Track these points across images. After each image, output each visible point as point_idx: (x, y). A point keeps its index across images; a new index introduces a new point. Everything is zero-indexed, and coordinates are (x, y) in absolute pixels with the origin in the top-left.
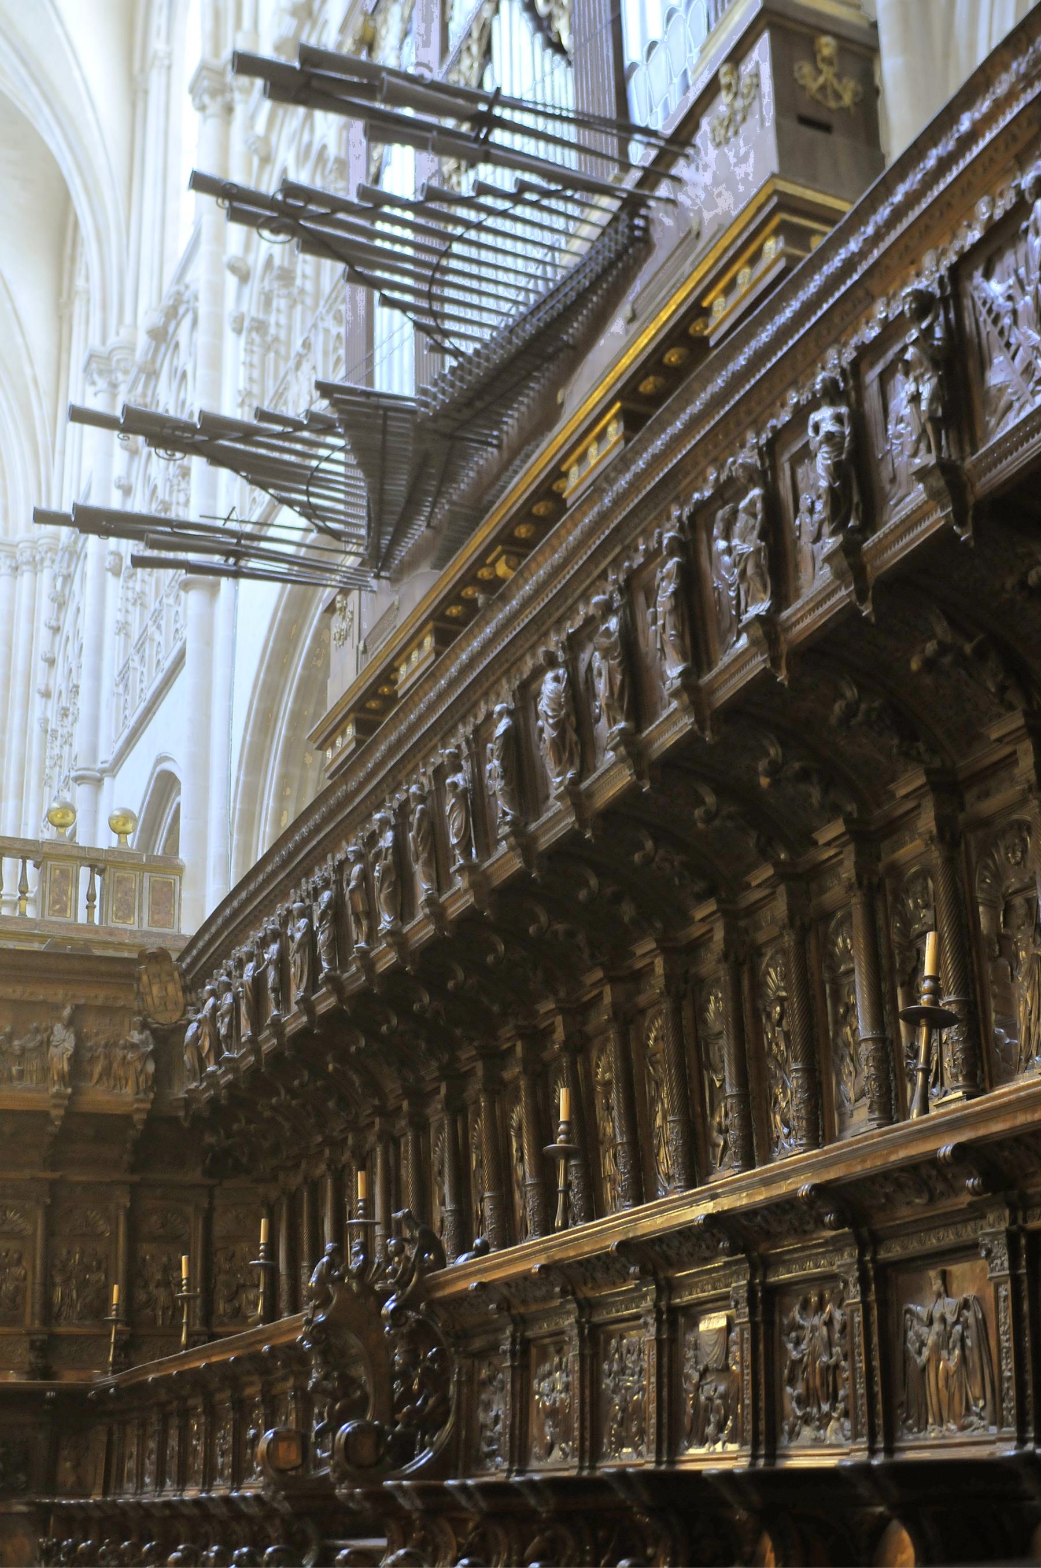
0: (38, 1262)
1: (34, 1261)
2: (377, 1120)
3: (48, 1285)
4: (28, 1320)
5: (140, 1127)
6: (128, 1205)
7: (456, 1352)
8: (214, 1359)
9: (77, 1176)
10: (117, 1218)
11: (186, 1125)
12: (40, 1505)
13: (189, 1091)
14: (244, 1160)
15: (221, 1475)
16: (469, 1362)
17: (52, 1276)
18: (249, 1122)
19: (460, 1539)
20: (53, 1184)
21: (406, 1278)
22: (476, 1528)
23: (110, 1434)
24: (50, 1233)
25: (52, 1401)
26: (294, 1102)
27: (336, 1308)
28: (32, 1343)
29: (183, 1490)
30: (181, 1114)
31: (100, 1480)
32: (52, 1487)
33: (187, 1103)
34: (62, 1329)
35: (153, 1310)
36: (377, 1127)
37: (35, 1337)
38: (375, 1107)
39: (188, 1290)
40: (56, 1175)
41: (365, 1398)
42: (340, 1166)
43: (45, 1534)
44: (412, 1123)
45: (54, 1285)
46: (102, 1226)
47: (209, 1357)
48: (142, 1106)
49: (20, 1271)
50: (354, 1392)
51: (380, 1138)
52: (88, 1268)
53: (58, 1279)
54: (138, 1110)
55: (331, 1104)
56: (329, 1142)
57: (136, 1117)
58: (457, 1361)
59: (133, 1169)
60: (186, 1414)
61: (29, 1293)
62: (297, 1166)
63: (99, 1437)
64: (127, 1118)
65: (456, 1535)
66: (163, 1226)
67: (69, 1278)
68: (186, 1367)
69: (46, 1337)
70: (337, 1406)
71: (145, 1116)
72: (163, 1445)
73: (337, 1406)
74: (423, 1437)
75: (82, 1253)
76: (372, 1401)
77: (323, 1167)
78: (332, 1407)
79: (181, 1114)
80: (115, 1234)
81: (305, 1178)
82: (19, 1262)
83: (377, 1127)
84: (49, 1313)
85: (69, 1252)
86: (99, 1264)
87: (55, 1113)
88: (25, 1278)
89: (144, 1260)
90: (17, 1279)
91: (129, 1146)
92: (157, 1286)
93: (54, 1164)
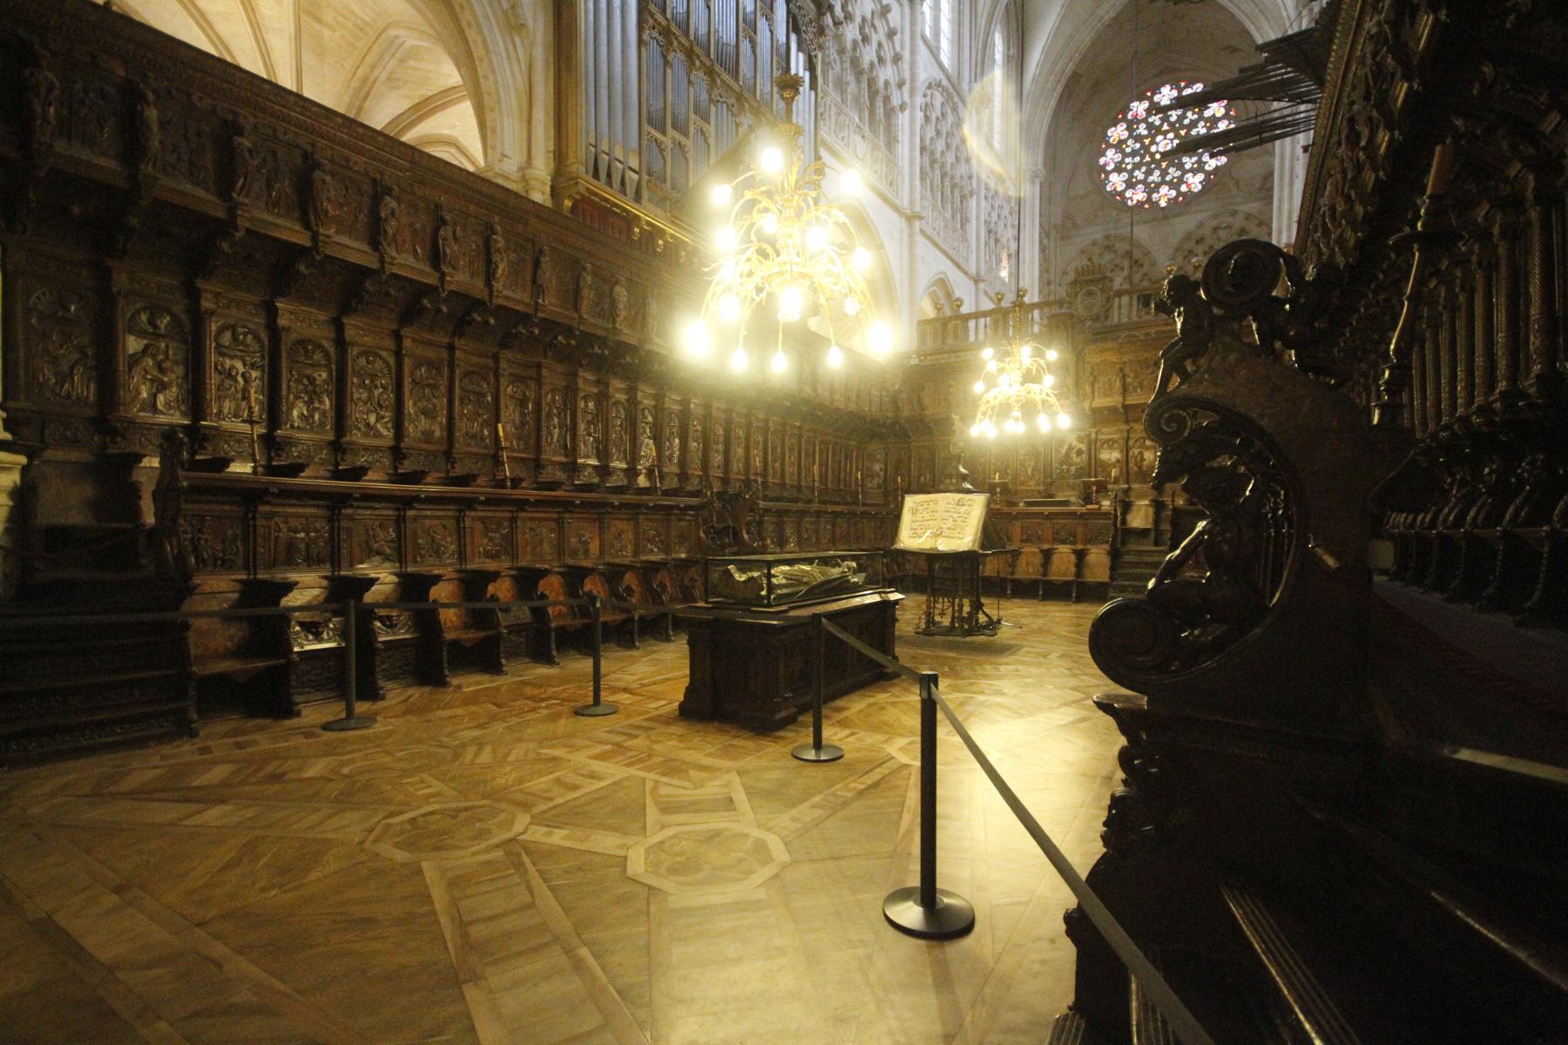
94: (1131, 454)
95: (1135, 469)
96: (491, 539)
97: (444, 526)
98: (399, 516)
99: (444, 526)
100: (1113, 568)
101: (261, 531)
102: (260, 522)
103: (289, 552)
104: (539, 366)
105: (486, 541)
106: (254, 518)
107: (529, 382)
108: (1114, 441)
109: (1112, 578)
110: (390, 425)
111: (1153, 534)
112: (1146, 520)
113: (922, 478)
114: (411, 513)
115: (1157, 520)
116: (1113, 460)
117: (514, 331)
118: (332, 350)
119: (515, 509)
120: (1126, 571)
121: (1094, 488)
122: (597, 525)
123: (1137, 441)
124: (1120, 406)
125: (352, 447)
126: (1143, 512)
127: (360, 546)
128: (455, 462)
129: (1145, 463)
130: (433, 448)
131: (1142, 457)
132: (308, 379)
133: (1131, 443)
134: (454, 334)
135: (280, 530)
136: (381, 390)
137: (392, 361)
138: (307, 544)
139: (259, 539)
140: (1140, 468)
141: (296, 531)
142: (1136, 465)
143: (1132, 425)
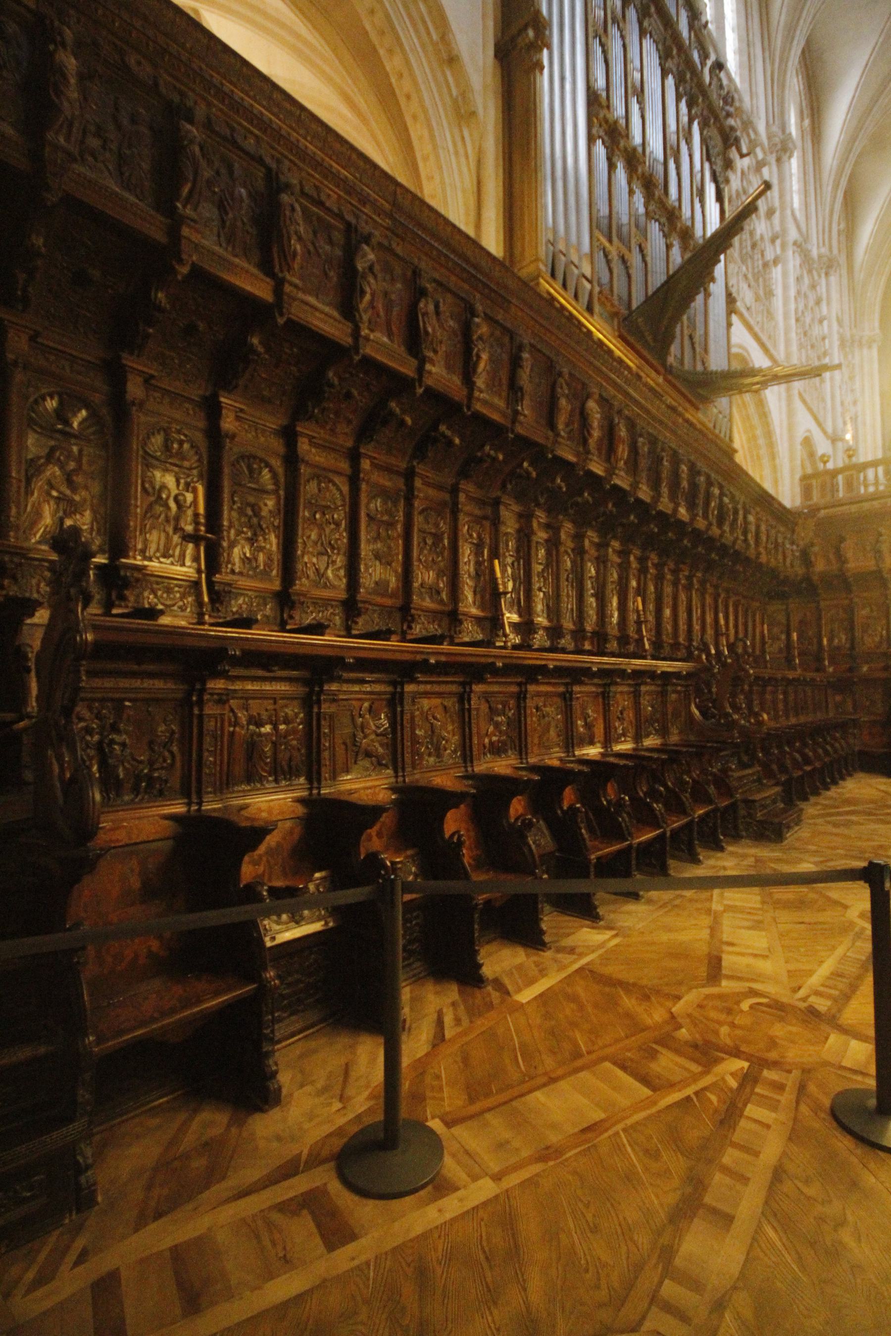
96: (497, 725)
97: (445, 707)
98: (393, 694)
99: (445, 707)
101: (209, 725)
102: (210, 709)
103: (249, 758)
104: (497, 503)
105: (491, 729)
106: (201, 703)
107: (484, 522)
110: (342, 573)
113: (836, 641)
114: (409, 688)
117: (479, 454)
118: (280, 471)
119: (568, 680)
122: (601, 700)
125: (302, 599)
127: (345, 743)
128: (413, 620)
130: (388, 602)
132: (253, 510)
134: (413, 457)
135: (236, 724)
136: (333, 526)
137: (345, 489)
138: (274, 744)
139: (207, 740)
141: (260, 724)
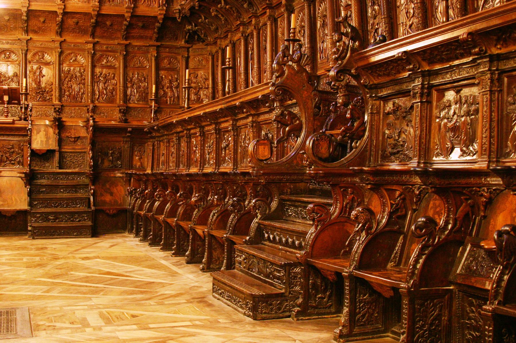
0: (121, 78)
1: (120, 77)
2: (268, 11)
3: (125, 88)
4: (118, 101)
5: (161, 21)
6: (156, 55)
7: (371, 97)
8: (207, 110)
9: (136, 43)
10: (151, 59)
11: (179, 20)
12: (127, 174)
13: (181, 5)
14: (202, 36)
15: (209, 163)
16: (377, 102)
17: (127, 84)
18: (205, 18)
19: (392, 202)
20: (127, 46)
21: (344, 55)
22: (400, 195)
23: (153, 146)
24: (125, 67)
25: (130, 132)
26: (227, 7)
27: (287, 78)
28: (120, 110)
29: (189, 169)
30: (177, 15)
31: (150, 164)
32: (131, 167)
33: (180, 11)
34: (131, 105)
35: (166, 97)
36: (268, 14)
37: (121, 108)
38: (267, 4)
39: (188, 85)
40: (128, 42)
41: (301, 125)
42: (247, 34)
43: (130, 186)
44: (287, 9)
45: (127, 88)
46: (146, 64)
47: (205, 109)
48: (162, 12)
49: (114, 82)
50: (296, 122)
51: (269, 19)
52: (140, 81)
53: (129, 85)
54: (160, 14)
55: (245, 6)
56: (243, 24)
57: (159, 17)
58: (370, 102)
59: (157, 40)
60: (189, 137)
61: (118, 90)
62: (226, 36)
63: (148, 146)
64: (155, 17)
65: (390, 200)
66: (169, 64)
67: (133, 85)
68: (192, 115)
69: (125, 108)
70: (287, 129)
71: (163, 17)
72: (178, 149)
73: (287, 129)
74: (351, 143)
75: (138, 74)
76: (304, 126)
77: (240, 35)
78: (285, 129)
79: (177, 15)
80: (151, 67)
81: (231, 41)
82: (114, 78)
83: (268, 14)
84: (126, 98)
85: (133, 74)
86: (145, 79)
87: (126, 15)
88: (116, 85)
89: (162, 77)
90: (113, 85)
91: (156, 30)
92: (167, 88)
93: (126, 39)
94: (29, 68)
95: (34, 85)
100: (30, 194)
108: (11, 52)
109: (30, 204)
111: (57, 155)
112: (47, 141)
115: (60, 142)
116: (11, 73)
120: (41, 196)
121: (6, 98)
123: (35, 55)
124: (25, 9)
126: (42, 134)
129: (44, 80)
131: (41, 72)
133: (29, 56)
140: (39, 83)
142: (35, 80)
143: (31, 36)
